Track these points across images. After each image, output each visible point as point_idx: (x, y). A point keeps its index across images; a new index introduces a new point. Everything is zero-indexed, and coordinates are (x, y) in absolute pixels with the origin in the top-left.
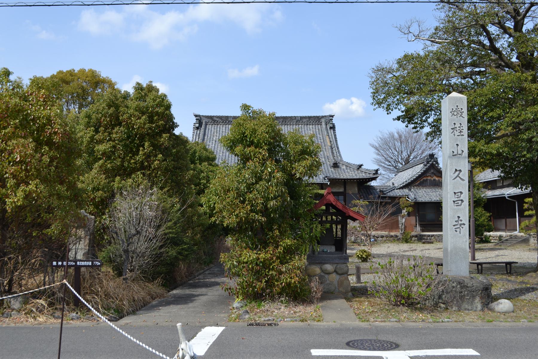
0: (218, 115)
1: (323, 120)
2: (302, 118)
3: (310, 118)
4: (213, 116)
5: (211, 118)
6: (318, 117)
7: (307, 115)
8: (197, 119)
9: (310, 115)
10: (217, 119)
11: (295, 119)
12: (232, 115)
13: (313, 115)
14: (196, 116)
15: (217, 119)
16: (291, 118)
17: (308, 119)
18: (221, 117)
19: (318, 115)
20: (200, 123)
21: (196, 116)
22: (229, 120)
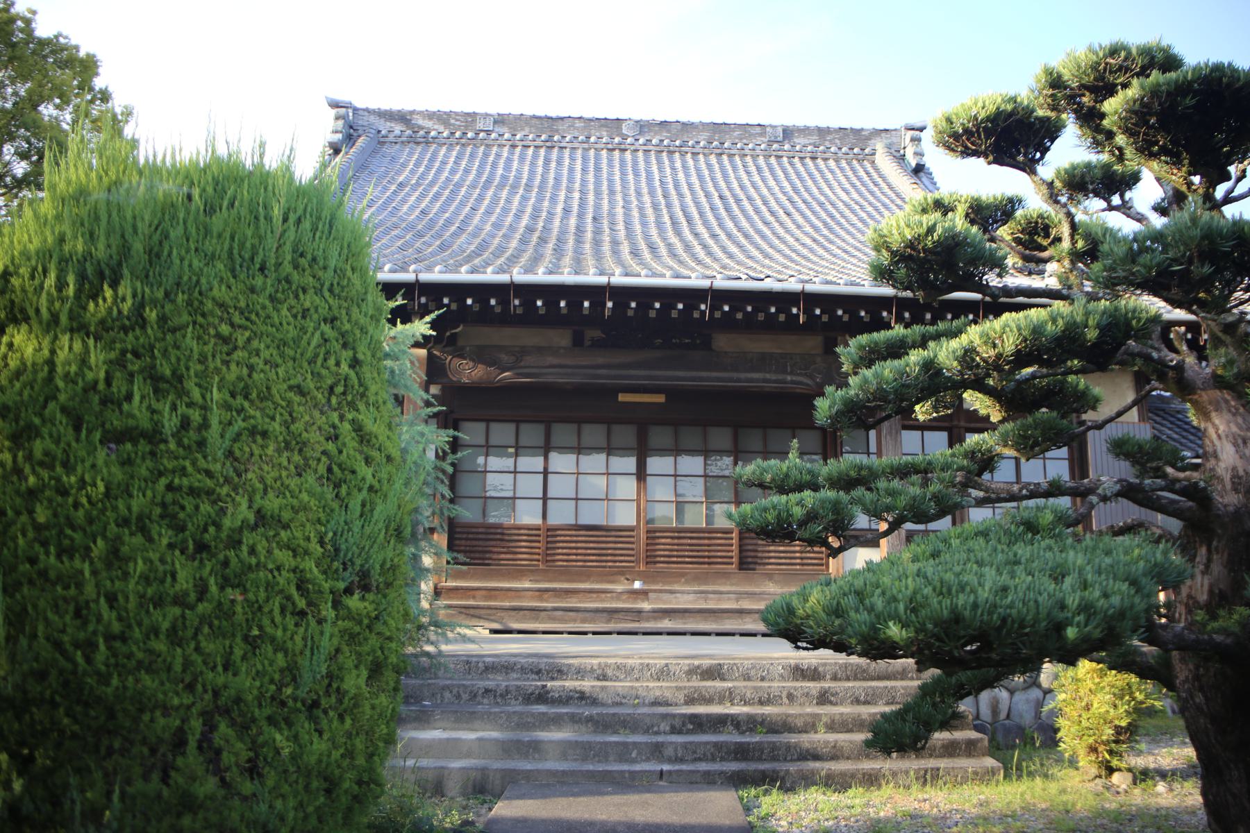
0: (433, 108)
1: (879, 146)
2: (788, 133)
3: (823, 132)
4: (412, 112)
5: (402, 117)
6: (857, 132)
7: (812, 123)
8: (337, 118)
9: (823, 124)
10: (428, 124)
11: (763, 134)
12: (494, 110)
13: (835, 124)
14: (335, 105)
15: (428, 124)
16: (745, 127)
17: (814, 139)
18: (442, 117)
19: (858, 127)
20: (350, 133)
21: (335, 105)
22: (480, 125)
